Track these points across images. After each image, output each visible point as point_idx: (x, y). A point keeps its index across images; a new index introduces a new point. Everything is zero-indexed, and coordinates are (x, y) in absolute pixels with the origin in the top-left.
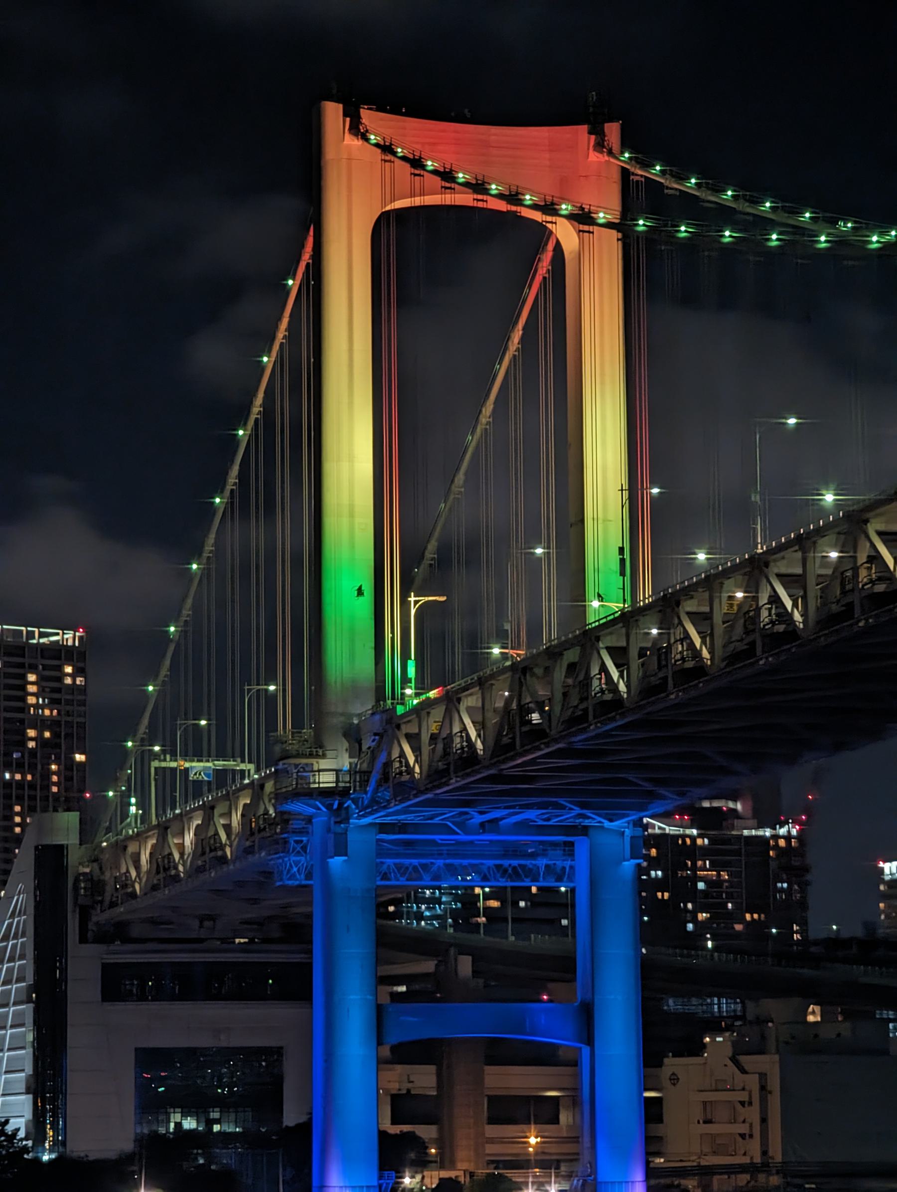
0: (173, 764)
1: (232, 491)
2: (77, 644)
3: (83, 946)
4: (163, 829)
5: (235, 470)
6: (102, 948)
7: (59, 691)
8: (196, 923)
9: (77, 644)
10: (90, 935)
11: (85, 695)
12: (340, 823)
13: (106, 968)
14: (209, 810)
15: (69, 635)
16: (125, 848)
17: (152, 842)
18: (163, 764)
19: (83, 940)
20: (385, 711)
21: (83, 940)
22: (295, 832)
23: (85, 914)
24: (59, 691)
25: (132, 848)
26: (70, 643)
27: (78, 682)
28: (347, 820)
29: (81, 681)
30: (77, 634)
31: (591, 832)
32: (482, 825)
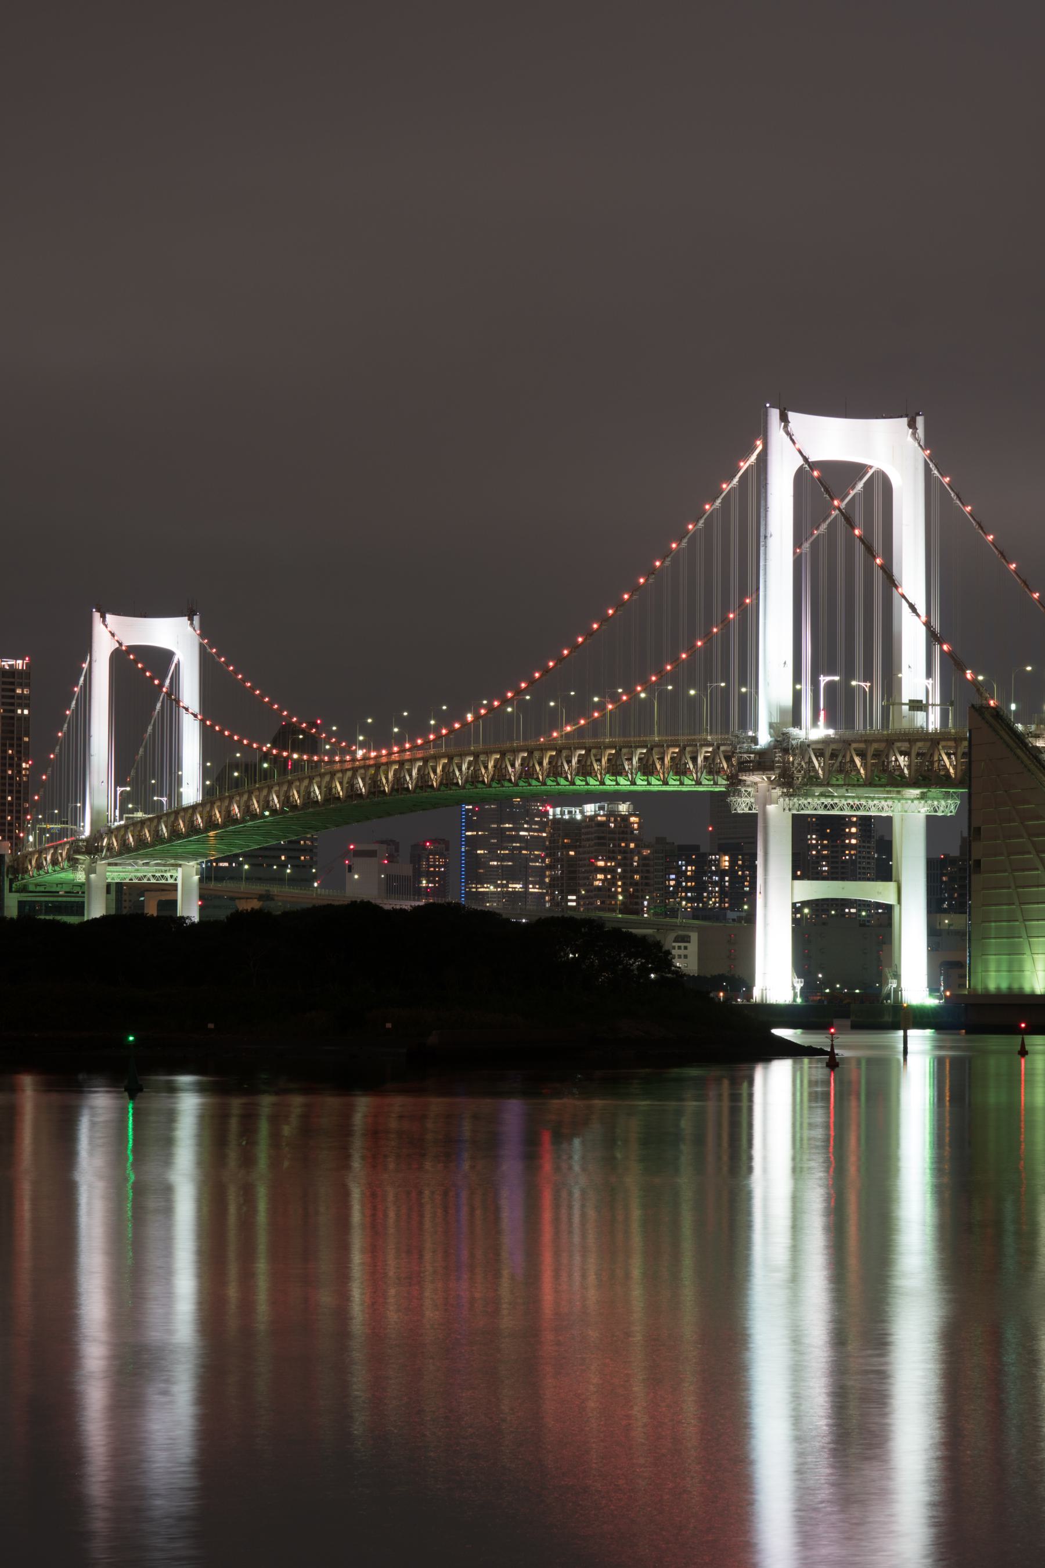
0: (45, 826)
1: (73, 710)
2: (24, 668)
3: (11, 894)
4: (40, 852)
5: (82, 679)
7: (13, 697)
8: (55, 885)
9: (24, 668)
10: (13, 889)
11: (29, 700)
12: (93, 863)
13: (20, 902)
14: (56, 848)
15: (20, 662)
16: (27, 857)
17: (36, 856)
18: (41, 826)
19: (11, 891)
20: (108, 826)
21: (11, 891)
22: (80, 864)
23: (11, 882)
24: (13, 697)
25: (29, 857)
26: (20, 668)
27: (25, 693)
28: (94, 861)
29: (27, 691)
30: (25, 661)
31: (183, 866)
32: (143, 864)
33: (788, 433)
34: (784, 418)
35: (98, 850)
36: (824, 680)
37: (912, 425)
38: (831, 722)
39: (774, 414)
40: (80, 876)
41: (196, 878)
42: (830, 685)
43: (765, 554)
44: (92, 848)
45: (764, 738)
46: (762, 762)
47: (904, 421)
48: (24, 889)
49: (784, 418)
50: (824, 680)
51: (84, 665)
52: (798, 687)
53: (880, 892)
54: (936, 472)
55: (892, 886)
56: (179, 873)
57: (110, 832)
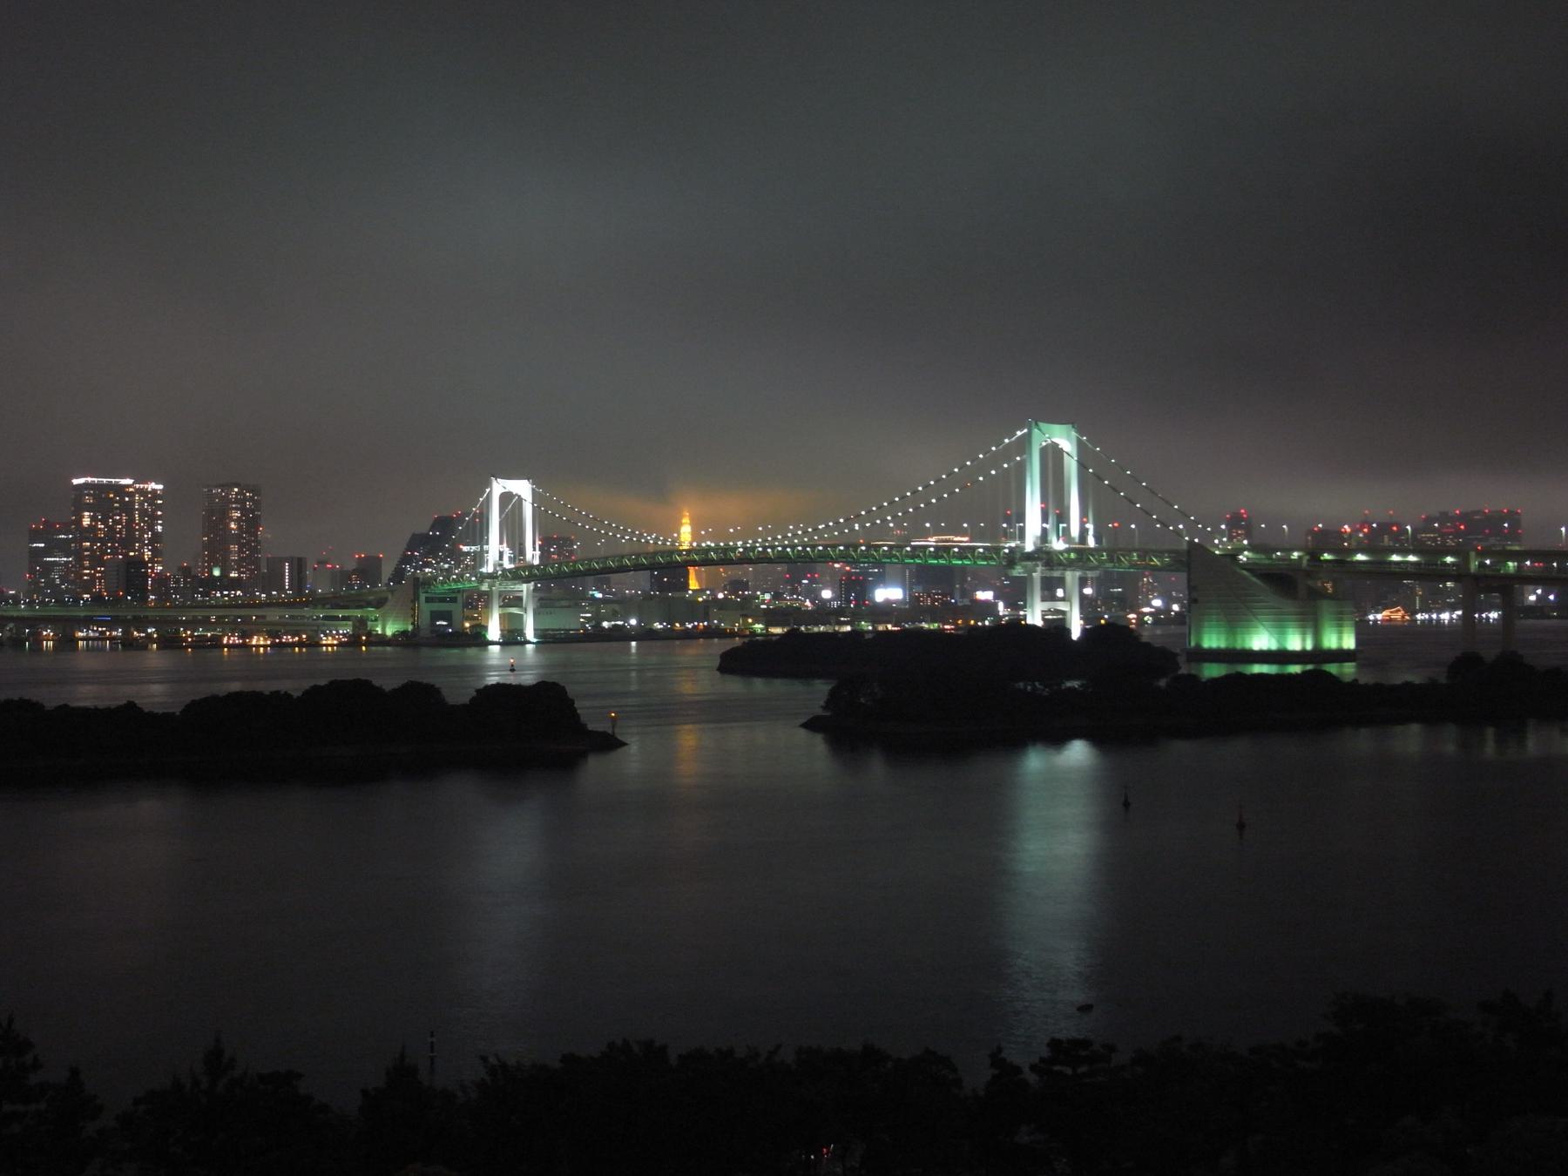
6: (424, 594)
33: (1040, 430)
34: (1036, 424)
35: (497, 577)
36: (1061, 525)
37: (1073, 427)
38: (1065, 542)
39: (1033, 424)
40: (485, 587)
41: (532, 588)
42: (1063, 528)
43: (1031, 477)
44: (492, 576)
45: (1029, 547)
46: (1028, 557)
47: (1070, 426)
48: (427, 592)
49: (1036, 424)
50: (1061, 525)
51: (481, 499)
52: (1045, 525)
53: (1062, 606)
54: (1090, 445)
55: (1069, 603)
56: (524, 587)
57: (504, 570)
